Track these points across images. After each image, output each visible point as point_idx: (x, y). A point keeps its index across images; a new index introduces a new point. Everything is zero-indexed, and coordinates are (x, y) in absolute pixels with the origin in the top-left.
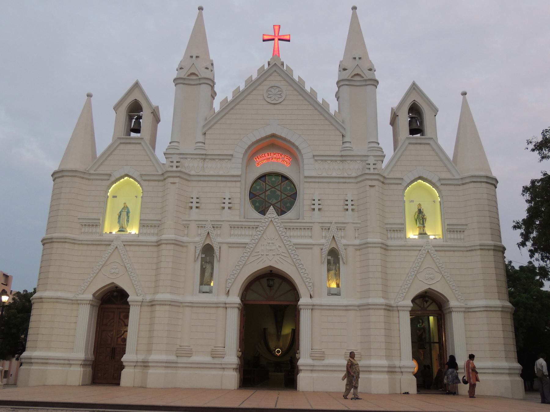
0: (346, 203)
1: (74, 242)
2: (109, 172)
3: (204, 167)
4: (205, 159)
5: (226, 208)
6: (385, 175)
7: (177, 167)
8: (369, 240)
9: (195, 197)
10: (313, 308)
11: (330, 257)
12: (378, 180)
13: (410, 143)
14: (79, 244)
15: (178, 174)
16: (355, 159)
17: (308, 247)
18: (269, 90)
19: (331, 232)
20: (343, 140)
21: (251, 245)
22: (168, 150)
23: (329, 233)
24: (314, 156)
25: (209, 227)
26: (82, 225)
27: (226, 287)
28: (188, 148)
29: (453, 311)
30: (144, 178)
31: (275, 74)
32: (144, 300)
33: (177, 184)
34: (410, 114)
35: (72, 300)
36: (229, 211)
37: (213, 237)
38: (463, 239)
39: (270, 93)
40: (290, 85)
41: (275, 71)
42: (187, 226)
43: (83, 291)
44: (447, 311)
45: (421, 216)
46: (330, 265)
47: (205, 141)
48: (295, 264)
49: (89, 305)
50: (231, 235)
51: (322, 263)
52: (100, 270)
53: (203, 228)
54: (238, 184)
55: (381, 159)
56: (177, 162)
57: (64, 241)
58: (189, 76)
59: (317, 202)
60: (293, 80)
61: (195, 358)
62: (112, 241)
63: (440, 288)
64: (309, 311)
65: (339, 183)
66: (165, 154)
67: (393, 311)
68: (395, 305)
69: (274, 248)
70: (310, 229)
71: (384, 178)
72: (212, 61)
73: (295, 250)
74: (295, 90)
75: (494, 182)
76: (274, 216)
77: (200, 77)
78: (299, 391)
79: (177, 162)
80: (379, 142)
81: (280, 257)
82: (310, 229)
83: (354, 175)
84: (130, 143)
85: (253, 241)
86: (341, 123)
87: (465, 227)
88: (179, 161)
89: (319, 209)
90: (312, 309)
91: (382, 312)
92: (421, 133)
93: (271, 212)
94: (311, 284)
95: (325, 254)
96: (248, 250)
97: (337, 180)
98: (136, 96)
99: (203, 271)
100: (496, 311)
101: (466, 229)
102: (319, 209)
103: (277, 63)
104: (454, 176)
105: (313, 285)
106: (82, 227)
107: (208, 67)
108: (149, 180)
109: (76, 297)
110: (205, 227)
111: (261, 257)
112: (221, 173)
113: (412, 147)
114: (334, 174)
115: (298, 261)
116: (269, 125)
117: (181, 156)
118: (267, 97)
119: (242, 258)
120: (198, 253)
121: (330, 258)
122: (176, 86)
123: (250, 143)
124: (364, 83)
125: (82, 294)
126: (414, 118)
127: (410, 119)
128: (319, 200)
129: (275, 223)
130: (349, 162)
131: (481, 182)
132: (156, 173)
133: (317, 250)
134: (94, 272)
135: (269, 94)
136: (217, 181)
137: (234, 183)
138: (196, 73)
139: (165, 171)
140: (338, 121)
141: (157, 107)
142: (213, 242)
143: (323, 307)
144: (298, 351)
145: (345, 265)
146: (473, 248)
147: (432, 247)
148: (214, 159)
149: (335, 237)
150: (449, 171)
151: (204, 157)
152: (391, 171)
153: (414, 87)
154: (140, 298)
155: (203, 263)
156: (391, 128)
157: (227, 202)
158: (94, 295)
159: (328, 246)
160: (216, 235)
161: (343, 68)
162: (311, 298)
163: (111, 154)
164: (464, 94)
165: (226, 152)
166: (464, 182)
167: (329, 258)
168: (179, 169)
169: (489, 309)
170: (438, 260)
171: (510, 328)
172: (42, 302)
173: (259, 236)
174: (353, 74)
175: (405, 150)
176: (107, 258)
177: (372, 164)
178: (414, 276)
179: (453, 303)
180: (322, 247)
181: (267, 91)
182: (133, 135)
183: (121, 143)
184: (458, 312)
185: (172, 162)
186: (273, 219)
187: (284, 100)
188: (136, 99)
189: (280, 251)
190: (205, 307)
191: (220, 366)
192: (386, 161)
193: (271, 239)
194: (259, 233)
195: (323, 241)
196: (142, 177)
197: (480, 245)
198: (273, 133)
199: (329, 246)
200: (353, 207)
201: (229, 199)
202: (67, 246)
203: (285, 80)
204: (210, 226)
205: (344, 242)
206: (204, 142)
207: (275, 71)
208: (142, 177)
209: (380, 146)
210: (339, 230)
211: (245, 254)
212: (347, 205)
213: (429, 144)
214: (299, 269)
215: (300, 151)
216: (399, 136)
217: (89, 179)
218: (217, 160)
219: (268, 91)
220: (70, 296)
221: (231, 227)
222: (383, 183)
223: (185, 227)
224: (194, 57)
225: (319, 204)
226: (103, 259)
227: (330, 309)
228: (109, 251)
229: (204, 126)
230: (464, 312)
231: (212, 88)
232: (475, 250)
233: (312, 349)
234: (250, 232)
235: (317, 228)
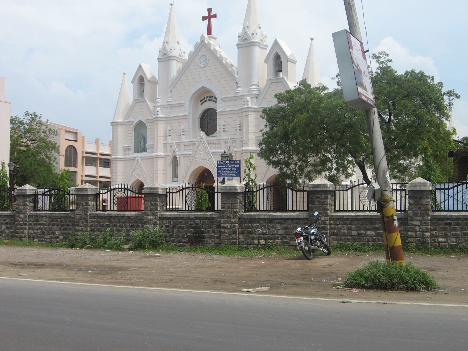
2: (132, 120)
4: (172, 107)
7: (158, 115)
13: (272, 83)
24: (222, 98)
50: (185, 150)
70: (219, 143)
77: (168, 56)
82: (219, 143)
89: (224, 131)
97: (232, 112)
108: (149, 123)
112: (180, 115)
114: (232, 109)
123: (192, 94)
124: (248, 45)
130: (239, 100)
136: (178, 119)
164: (312, 39)
174: (243, 40)
175: (269, 87)
183: (136, 103)
202: (118, 162)
205: (235, 149)
219: (200, 59)
235: (222, 142)
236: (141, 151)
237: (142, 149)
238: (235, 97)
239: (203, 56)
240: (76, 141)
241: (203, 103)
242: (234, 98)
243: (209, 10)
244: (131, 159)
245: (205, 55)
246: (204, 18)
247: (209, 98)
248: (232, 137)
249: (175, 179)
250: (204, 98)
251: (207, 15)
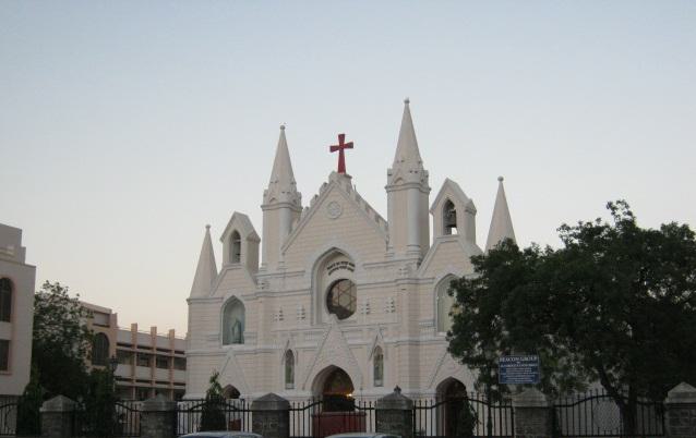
17: (360, 346)
24: (364, 265)
28: (272, 269)
165: (298, 270)
205: (386, 340)
236: (235, 343)
240: (108, 326)
243: (342, 137)
246: (333, 149)
248: (380, 321)
249: (290, 385)
251: (337, 144)
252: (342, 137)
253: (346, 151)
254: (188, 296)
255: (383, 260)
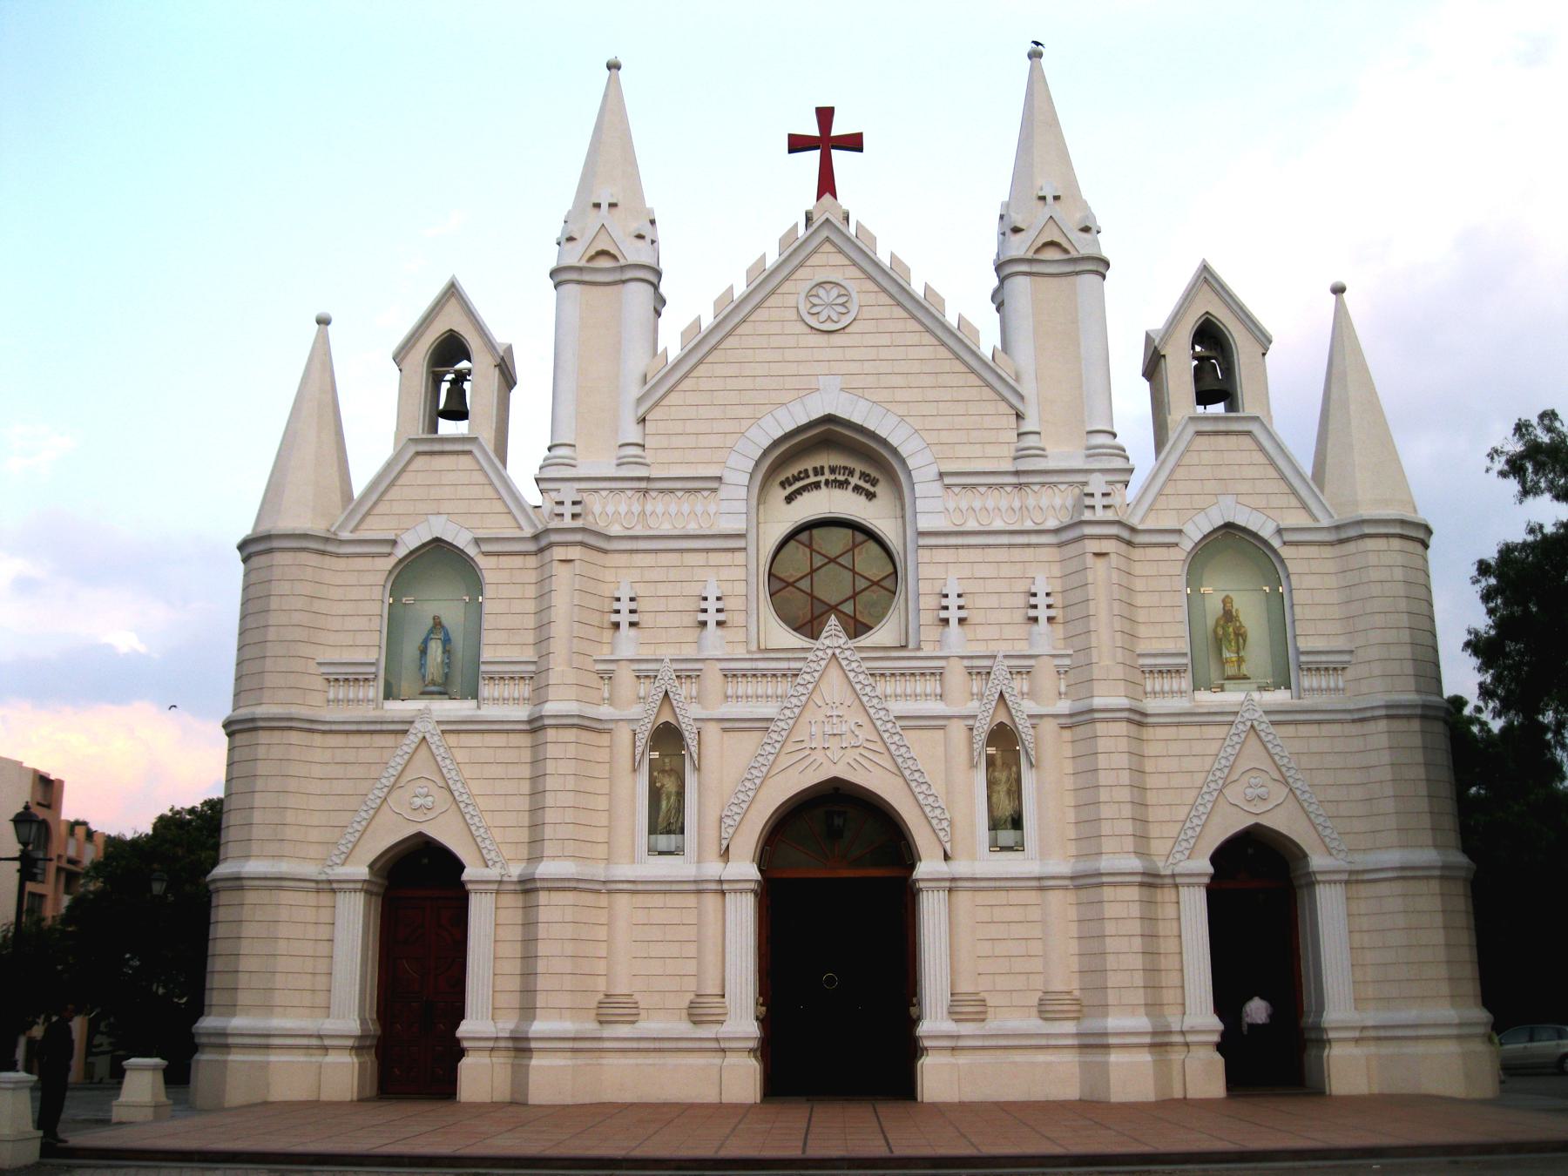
0: (1033, 601)
1: (311, 727)
3: (644, 513)
4: (646, 491)
5: (711, 625)
6: (1135, 521)
7: (574, 516)
8: (1098, 702)
9: (625, 594)
10: (952, 886)
11: (994, 749)
12: (1118, 538)
13: (1199, 433)
14: (324, 732)
15: (578, 537)
16: (1055, 479)
17: (936, 723)
18: (813, 292)
19: (996, 682)
20: (1018, 428)
21: (782, 724)
22: (544, 470)
23: (990, 684)
24: (941, 475)
25: (666, 678)
26: (327, 679)
27: (721, 839)
29: (1319, 882)
30: (486, 548)
31: (827, 247)
32: (505, 879)
33: (577, 563)
34: (1198, 348)
35: (317, 882)
36: (720, 632)
37: (680, 704)
38: (1343, 690)
39: (815, 302)
40: (870, 277)
41: (828, 239)
42: (607, 676)
43: (343, 856)
44: (1303, 881)
45: (1231, 630)
46: (994, 771)
47: (644, 440)
48: (901, 772)
49: (363, 894)
51: (973, 766)
52: (386, 799)
53: (652, 680)
54: (740, 558)
55: (1122, 478)
56: (574, 503)
57: (284, 725)
58: (591, 259)
59: (953, 602)
60: (877, 264)
61: (650, 1026)
62: (412, 722)
63: (1282, 821)
64: (943, 895)
65: (1010, 546)
66: (537, 480)
67: (1162, 886)
68: (1169, 872)
69: (844, 728)
71: (1133, 530)
72: (651, 211)
73: (901, 732)
74: (885, 290)
75: (1421, 535)
76: (841, 641)
77: (622, 262)
78: (922, 1102)
79: (574, 503)
80: (1116, 430)
81: (860, 754)
82: (938, 674)
83: (1052, 523)
84: (442, 453)
85: (787, 712)
86: (1012, 382)
87: (1346, 658)
88: (579, 499)
89: (961, 621)
90: (950, 890)
91: (1134, 893)
92: (1227, 401)
93: (833, 632)
94: (945, 824)
95: (981, 743)
96: (775, 736)
97: (1005, 540)
98: (453, 320)
99: (655, 794)
100: (1427, 878)
101: (1349, 662)
102: (961, 621)
103: (832, 218)
104: (1316, 519)
105: (951, 823)
106: (330, 686)
107: (643, 233)
108: (498, 554)
109: (327, 874)
110: (656, 676)
111: (810, 754)
112: (692, 528)
113: (1203, 442)
114: (998, 525)
115: (910, 762)
116: (818, 389)
117: (583, 485)
118: (809, 313)
119: (760, 759)
120: (640, 749)
121: (994, 752)
122: (559, 288)
123: (766, 443)
125: (343, 865)
126: (1209, 358)
127: (1196, 362)
128: (959, 596)
129: (844, 663)
130: (1036, 488)
131: (1387, 536)
132: (517, 534)
133: (958, 730)
134: (367, 805)
135: (815, 305)
136: (681, 551)
137: (730, 555)
138: (612, 252)
139: (540, 527)
140: (1004, 375)
141: (509, 349)
142: (680, 718)
143: (977, 884)
144: (915, 1000)
145: (1034, 769)
146: (1368, 714)
147: (1262, 713)
148: (672, 491)
149: (1007, 696)
150: (1305, 507)
151: (643, 485)
152: (1150, 509)
153: (1206, 278)
154: (493, 873)
155: (656, 774)
156: (1145, 385)
157: (712, 610)
158: (371, 866)
159: (988, 719)
160: (685, 698)
161: (1012, 226)
162: (945, 860)
163: (392, 484)
164: (1338, 290)
166: (1344, 535)
167: (992, 750)
168: (579, 523)
169: (1409, 874)
170: (1278, 749)
171: (1463, 920)
172: (241, 888)
173: (803, 698)
174: (1040, 243)
175: (1187, 450)
176: (400, 768)
177: (1098, 496)
178: (1215, 794)
179: (1318, 861)
180: (971, 722)
181: (807, 296)
182: (447, 427)
183: (418, 453)
184: (1330, 882)
185: (561, 503)
186: (837, 651)
187: (855, 319)
188: (451, 330)
189: (860, 737)
190: (665, 892)
191: (714, 1045)
192: (1137, 481)
193: (834, 706)
194: (800, 689)
195: (973, 707)
196: (479, 547)
197: (1387, 707)
198: (829, 414)
199: (991, 720)
200: (1052, 612)
201: (718, 599)
202: (294, 737)
203: (855, 264)
204: (669, 674)
205: (1029, 706)
206: (641, 442)
207: (828, 239)
208: (479, 547)
209: (1119, 441)
210: (1014, 676)
211: (768, 748)
212: (1035, 607)
213: (1248, 433)
214: (913, 784)
215: (903, 462)
216: (1170, 414)
217: (338, 555)
218: (680, 494)
220: (310, 870)
221: (725, 675)
222: (1129, 543)
223: (602, 677)
224: (605, 206)
225: (960, 608)
226: (391, 770)
227: (995, 889)
228: (405, 748)
229: (640, 401)
230: (1347, 882)
231: (656, 287)
232: (1374, 718)
233: (952, 994)
234: (783, 687)
235: (956, 673)
237: (433, 683)
238: (1017, 473)
239: (828, 286)
241: (799, 492)
242: (1013, 480)
243: (825, 116)
244: (378, 727)
245: (837, 284)
247: (827, 476)
249: (663, 841)
250: (806, 471)
251: (813, 130)
252: (825, 116)
253: (837, 156)
254: (246, 529)
255: (1008, 466)
